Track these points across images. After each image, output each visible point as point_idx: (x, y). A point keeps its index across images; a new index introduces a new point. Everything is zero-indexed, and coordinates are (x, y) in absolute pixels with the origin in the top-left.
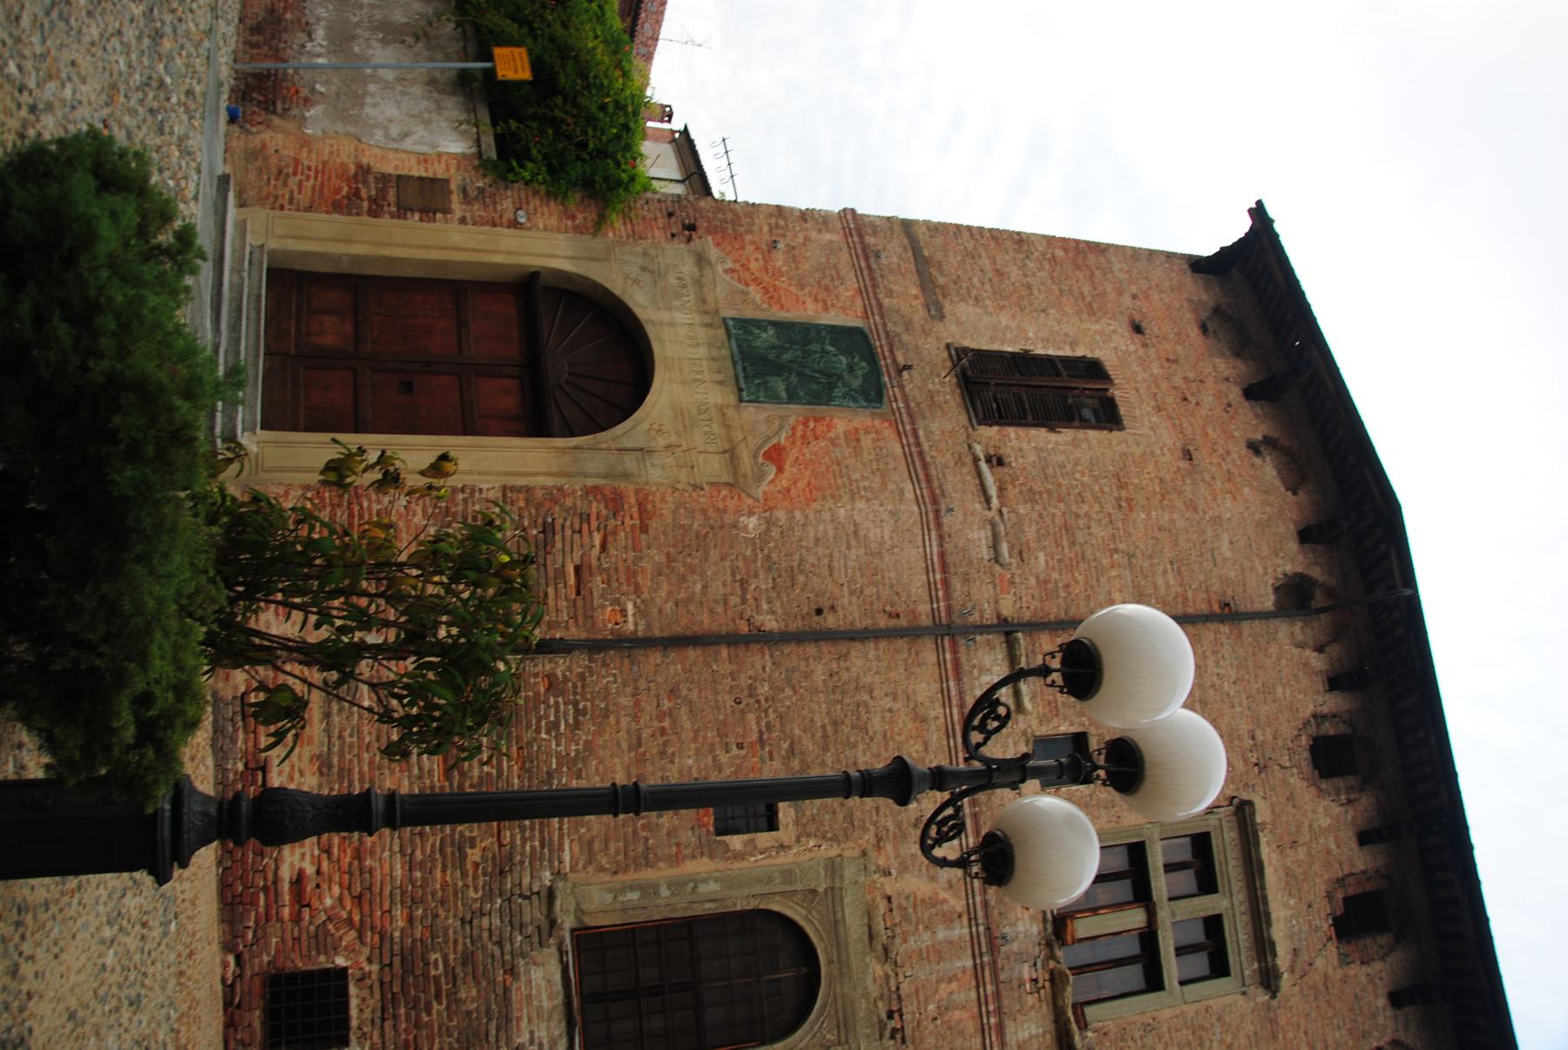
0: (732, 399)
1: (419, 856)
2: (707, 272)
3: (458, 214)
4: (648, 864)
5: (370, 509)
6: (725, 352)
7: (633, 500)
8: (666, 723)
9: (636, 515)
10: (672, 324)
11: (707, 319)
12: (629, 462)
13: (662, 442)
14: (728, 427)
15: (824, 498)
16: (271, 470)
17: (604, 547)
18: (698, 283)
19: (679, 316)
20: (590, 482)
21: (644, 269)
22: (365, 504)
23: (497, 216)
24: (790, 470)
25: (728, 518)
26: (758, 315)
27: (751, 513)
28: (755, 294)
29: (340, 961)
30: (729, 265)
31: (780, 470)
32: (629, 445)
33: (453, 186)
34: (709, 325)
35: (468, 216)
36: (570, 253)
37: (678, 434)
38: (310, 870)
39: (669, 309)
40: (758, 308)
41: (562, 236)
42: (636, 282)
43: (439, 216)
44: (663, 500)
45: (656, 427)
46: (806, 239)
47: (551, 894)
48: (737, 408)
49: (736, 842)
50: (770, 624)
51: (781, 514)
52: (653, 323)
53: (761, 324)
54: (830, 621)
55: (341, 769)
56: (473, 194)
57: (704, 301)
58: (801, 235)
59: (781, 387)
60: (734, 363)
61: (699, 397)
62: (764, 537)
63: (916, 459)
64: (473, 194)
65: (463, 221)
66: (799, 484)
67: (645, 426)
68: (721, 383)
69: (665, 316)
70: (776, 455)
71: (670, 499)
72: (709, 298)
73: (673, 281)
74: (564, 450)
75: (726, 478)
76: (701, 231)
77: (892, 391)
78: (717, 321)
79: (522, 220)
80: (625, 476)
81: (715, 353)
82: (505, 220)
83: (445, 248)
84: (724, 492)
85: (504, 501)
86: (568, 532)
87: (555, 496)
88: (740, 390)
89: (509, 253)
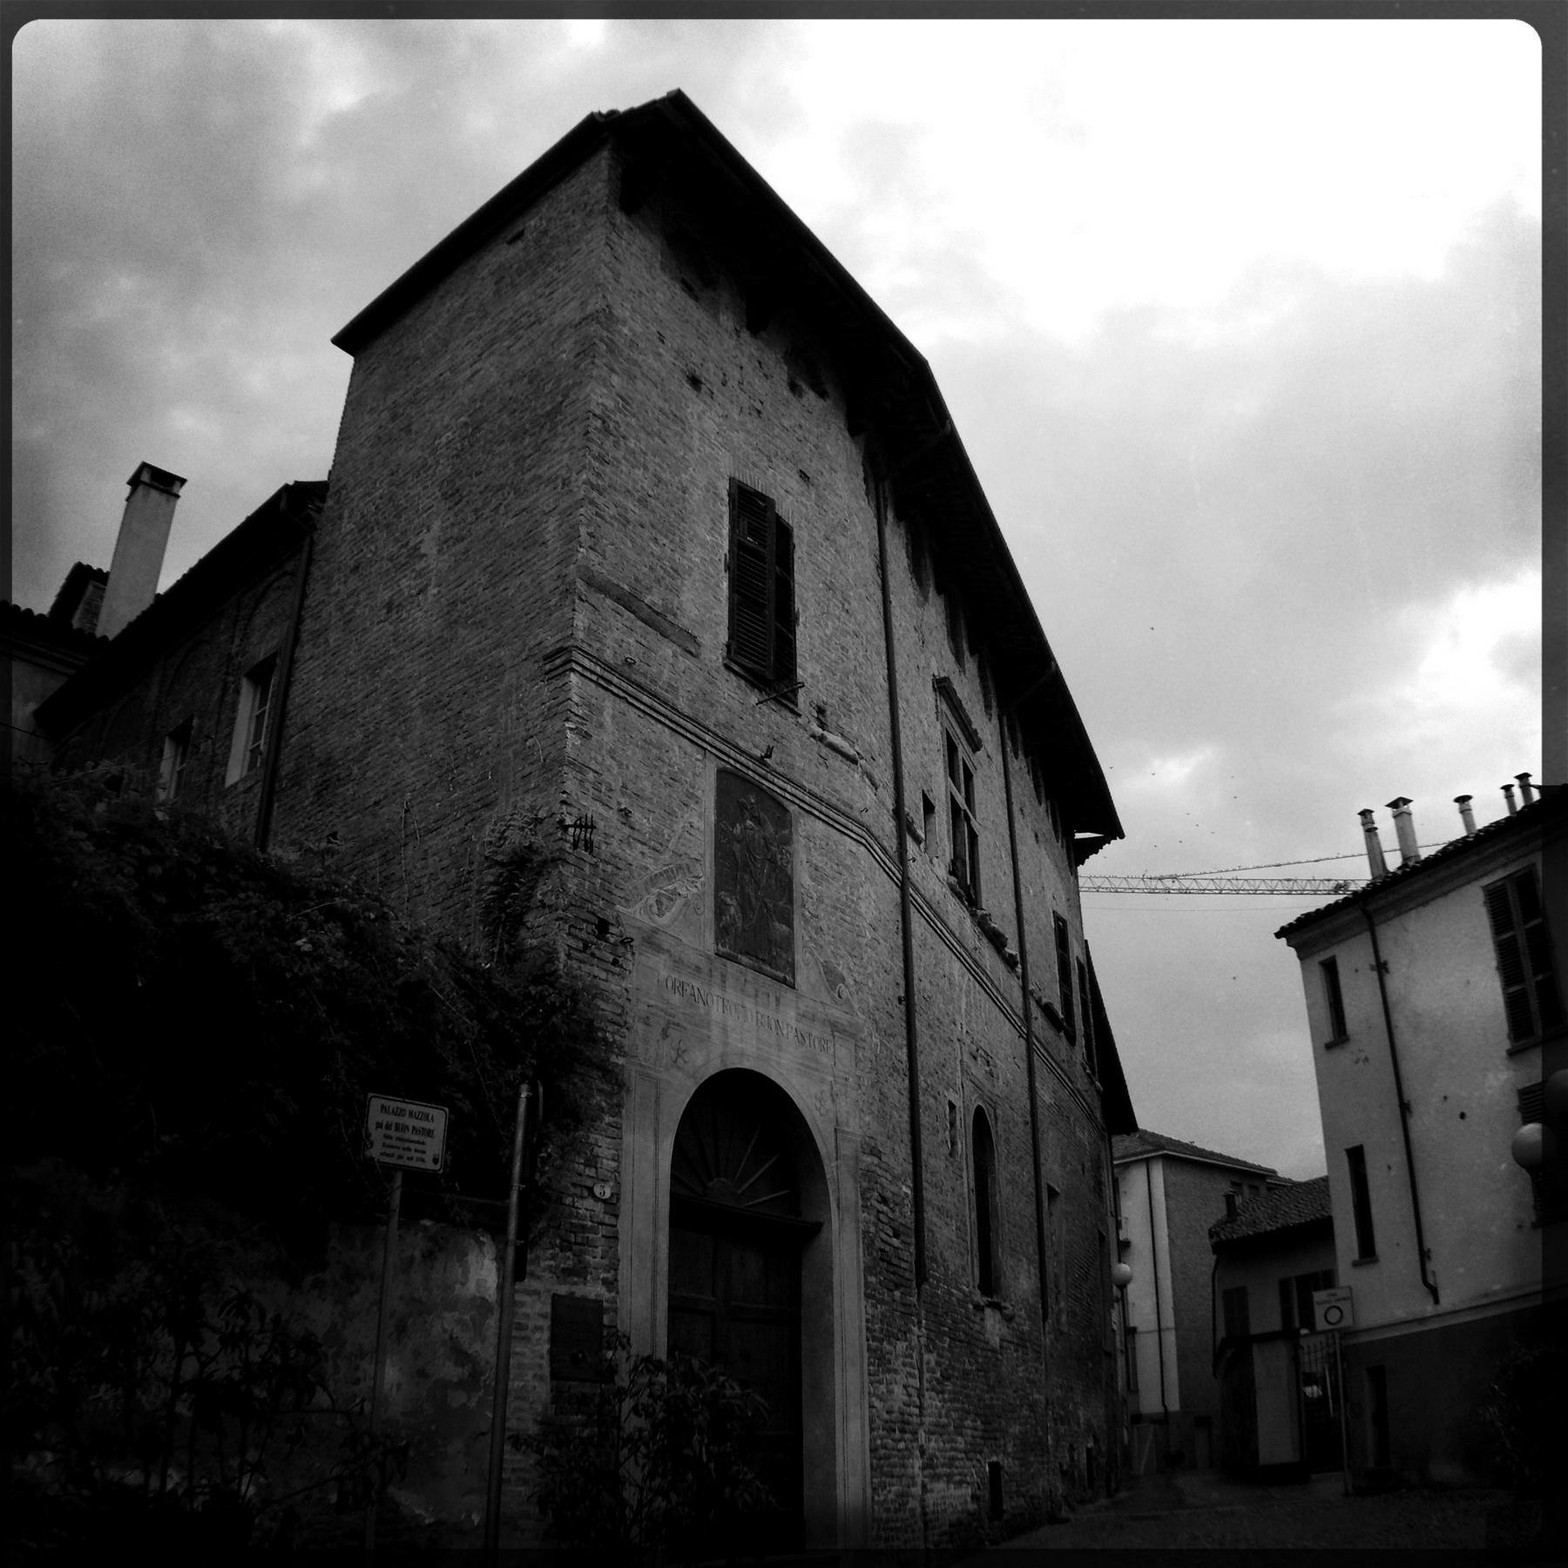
18: (678, 963)
19: (716, 1012)
21: (665, 1035)
26: (710, 901)
28: (686, 889)
30: (652, 901)
40: (700, 896)
42: (680, 1053)
46: (612, 753)
53: (720, 909)
57: (698, 969)
58: (609, 761)
63: (832, 814)
69: (715, 1032)
72: (693, 958)
73: (676, 999)
76: (609, 915)
77: (776, 785)
78: (719, 962)
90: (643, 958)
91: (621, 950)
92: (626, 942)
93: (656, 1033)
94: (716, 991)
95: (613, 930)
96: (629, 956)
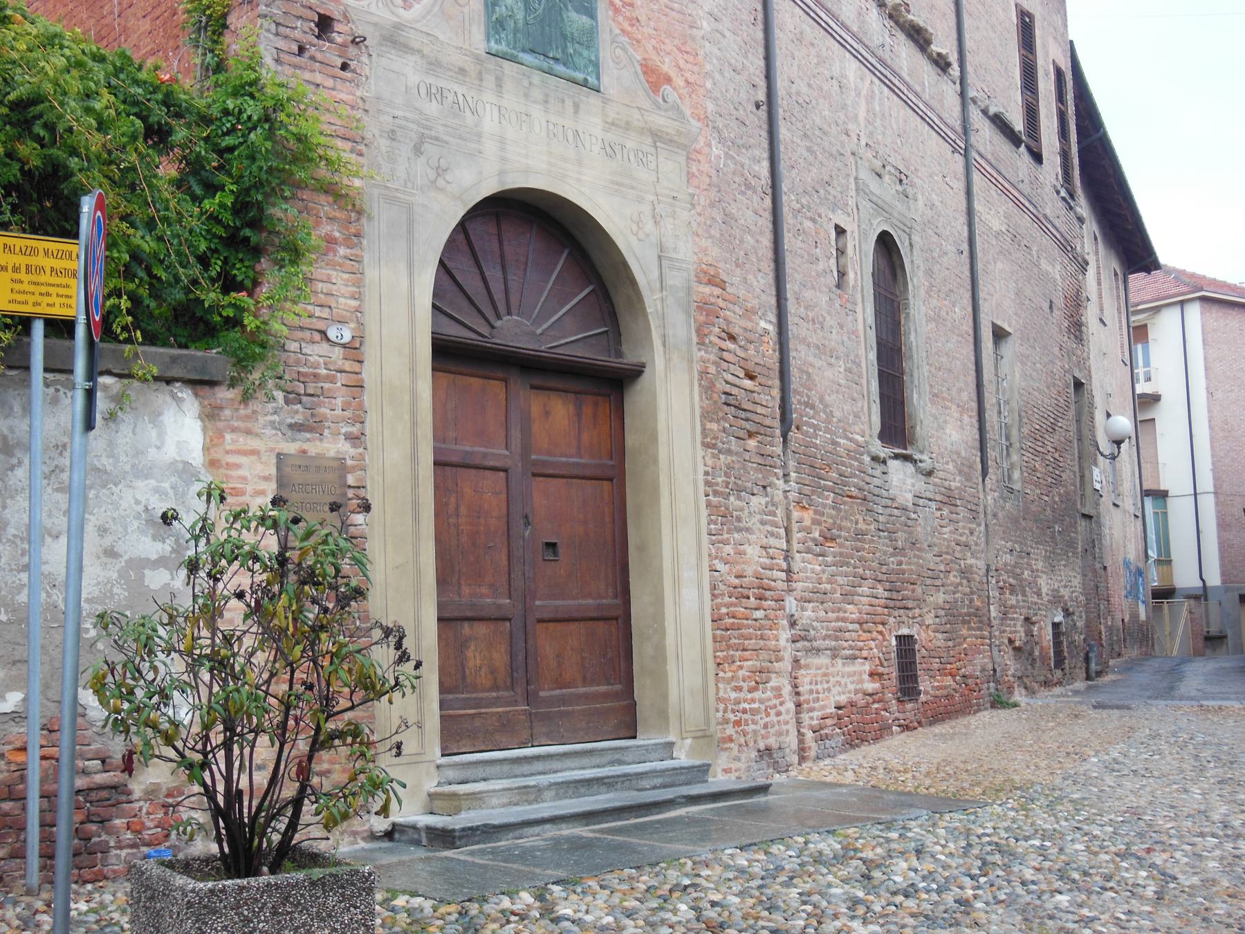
0: (593, 100)
1: (861, 571)
2: (415, 40)
3: (345, 448)
4: (859, 365)
5: (728, 606)
6: (537, 77)
7: (707, 290)
8: (810, 314)
9: (717, 291)
10: (502, 141)
11: (489, 80)
12: (675, 279)
13: (649, 226)
14: (628, 126)
15: (693, 39)
16: (707, 722)
17: (732, 338)
18: (434, 65)
19: (490, 122)
20: (695, 339)
21: (418, 150)
22: (724, 610)
23: (341, 379)
24: (667, 67)
25: (715, 179)
27: (709, 145)
29: (894, 643)
31: (668, 80)
32: (656, 274)
33: (291, 448)
34: (499, 84)
35: (343, 431)
36: (402, 267)
37: (640, 200)
38: (867, 667)
39: (480, 135)
41: (371, 273)
42: (440, 171)
43: (351, 480)
44: (705, 251)
45: (635, 228)
47: (875, 459)
48: (606, 101)
49: (851, 275)
50: (764, 168)
51: (710, 107)
52: (501, 173)
54: (761, 96)
55: (837, 639)
56: (298, 414)
57: (462, 71)
59: (576, 20)
60: (550, 72)
61: (597, 148)
62: (721, 140)
64: (298, 414)
65: (356, 439)
66: (681, 63)
67: (634, 240)
68: (576, 107)
69: (490, 147)
70: (655, 79)
71: (704, 243)
72: (457, 59)
73: (433, 108)
74: (668, 361)
75: (682, 160)
79: (347, 338)
80: (689, 290)
81: (537, 94)
82: (348, 366)
83: (415, 477)
84: (694, 169)
85: (714, 446)
86: (730, 378)
87: (708, 388)
88: (585, 84)
89: (413, 370)
90: (384, 62)
91: (352, 51)
92: (357, 41)
93: (405, 151)
94: (489, 96)
95: (338, 27)
96: (364, 59)
